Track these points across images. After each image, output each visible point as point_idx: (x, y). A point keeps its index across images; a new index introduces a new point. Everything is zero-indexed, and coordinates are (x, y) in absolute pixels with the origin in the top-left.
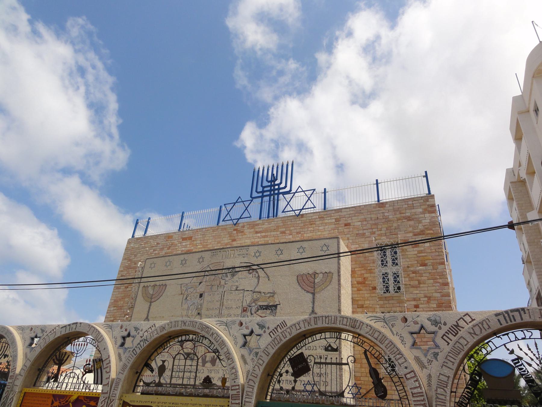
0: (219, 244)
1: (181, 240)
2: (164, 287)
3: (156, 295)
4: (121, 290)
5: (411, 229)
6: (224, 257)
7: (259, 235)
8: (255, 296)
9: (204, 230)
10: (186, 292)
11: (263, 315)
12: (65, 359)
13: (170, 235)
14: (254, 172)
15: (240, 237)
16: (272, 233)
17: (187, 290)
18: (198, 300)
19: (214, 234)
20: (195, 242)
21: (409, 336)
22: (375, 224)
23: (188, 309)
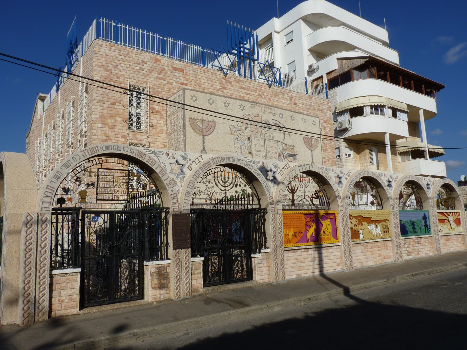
0: (212, 88)
1: (172, 69)
2: (213, 124)
3: (207, 129)
4: (105, 105)
5: (323, 118)
6: (260, 111)
7: (243, 90)
10: (235, 133)
11: (290, 160)
12: (296, 189)
16: (253, 93)
17: (235, 131)
18: (247, 142)
20: (188, 77)
21: (169, 165)
22: (308, 109)
23: (241, 148)
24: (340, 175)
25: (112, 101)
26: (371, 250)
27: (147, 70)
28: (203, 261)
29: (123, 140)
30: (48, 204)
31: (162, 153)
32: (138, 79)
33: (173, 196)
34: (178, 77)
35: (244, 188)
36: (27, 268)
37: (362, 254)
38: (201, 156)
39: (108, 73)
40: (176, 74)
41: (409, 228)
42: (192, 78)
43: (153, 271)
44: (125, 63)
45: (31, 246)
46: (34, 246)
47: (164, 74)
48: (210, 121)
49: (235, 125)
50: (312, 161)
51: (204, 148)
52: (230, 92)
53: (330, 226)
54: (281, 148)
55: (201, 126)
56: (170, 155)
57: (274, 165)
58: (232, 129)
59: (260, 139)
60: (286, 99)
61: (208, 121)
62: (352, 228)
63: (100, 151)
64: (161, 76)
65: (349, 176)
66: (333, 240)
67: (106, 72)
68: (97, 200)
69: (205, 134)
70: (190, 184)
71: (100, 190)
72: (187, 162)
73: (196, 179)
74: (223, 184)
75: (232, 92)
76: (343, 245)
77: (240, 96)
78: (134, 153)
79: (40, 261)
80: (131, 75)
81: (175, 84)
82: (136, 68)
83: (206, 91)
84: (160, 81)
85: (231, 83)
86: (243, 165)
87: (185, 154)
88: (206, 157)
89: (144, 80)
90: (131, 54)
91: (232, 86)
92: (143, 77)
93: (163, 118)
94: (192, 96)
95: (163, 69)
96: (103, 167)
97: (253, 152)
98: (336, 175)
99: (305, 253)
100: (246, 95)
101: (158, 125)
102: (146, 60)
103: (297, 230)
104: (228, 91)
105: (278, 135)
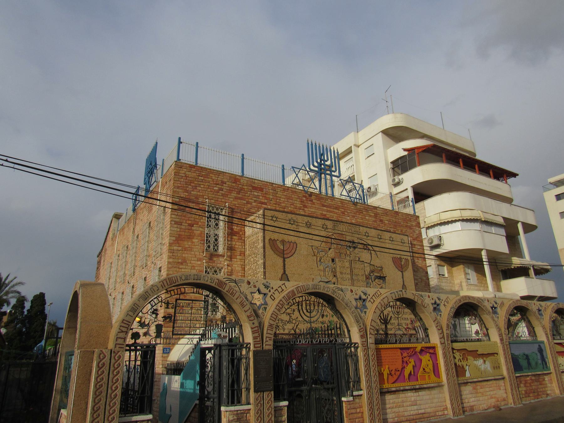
0: (292, 206)
1: (251, 188)
7: (325, 208)
8: (372, 268)
9: (274, 185)
12: (389, 318)
13: (238, 177)
14: (308, 143)
15: (310, 205)
16: (335, 210)
19: (285, 194)
23: (324, 270)
24: (438, 302)
25: (190, 222)
26: (481, 390)
27: (226, 190)
28: (288, 407)
29: (199, 263)
30: (123, 340)
31: (243, 282)
32: (216, 199)
33: (255, 329)
34: (258, 197)
35: (331, 319)
36: (95, 415)
37: (470, 396)
38: (284, 284)
39: (187, 194)
40: (256, 194)
41: (524, 363)
42: (271, 197)
43: (231, 418)
44: (204, 184)
45: (101, 389)
46: (104, 388)
47: (244, 194)
48: (291, 242)
49: (317, 246)
50: (404, 284)
51: (285, 271)
52: (312, 210)
54: (368, 270)
55: (282, 247)
56: (252, 284)
58: (315, 250)
59: (345, 261)
60: (370, 216)
61: (288, 242)
62: (455, 364)
63: (179, 281)
64: (239, 196)
65: (448, 303)
67: (185, 193)
68: (173, 334)
69: (285, 256)
70: (273, 316)
71: (178, 324)
72: (270, 291)
73: (279, 310)
74: (308, 314)
75: (314, 210)
77: (322, 214)
78: (215, 283)
79: (110, 406)
80: (209, 195)
81: (254, 204)
82: (215, 188)
83: (286, 210)
84: (239, 201)
85: (312, 201)
86: (329, 293)
87: (267, 282)
88: (291, 286)
89: (223, 200)
90: (211, 175)
91: (314, 204)
92: (222, 197)
93: (241, 239)
94: (272, 217)
95: (242, 189)
96: (181, 298)
97: (338, 274)
98: (433, 302)
100: (328, 213)
101: (236, 246)
102: (225, 180)
104: (309, 209)
105: (365, 256)
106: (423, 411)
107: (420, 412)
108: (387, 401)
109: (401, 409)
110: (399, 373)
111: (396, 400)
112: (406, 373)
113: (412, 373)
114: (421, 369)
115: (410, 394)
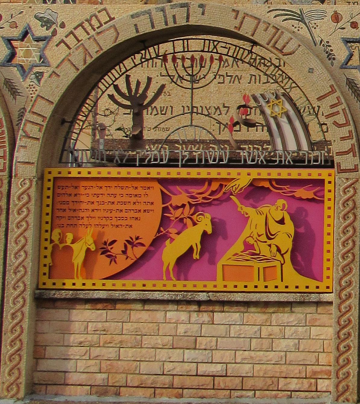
53: (289, 227)
57: (40, 19)
66: (293, 279)
76: (336, 301)
99: (144, 316)
103: (121, 236)
106: (217, 369)
107: (203, 369)
108: (76, 327)
109: (128, 353)
110: (139, 251)
111: (112, 326)
112: (171, 252)
113: (196, 256)
114: (238, 247)
115: (173, 314)
